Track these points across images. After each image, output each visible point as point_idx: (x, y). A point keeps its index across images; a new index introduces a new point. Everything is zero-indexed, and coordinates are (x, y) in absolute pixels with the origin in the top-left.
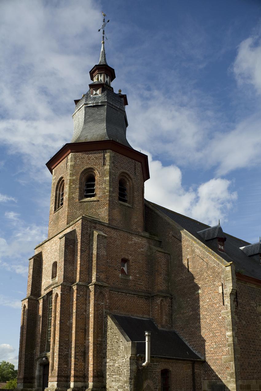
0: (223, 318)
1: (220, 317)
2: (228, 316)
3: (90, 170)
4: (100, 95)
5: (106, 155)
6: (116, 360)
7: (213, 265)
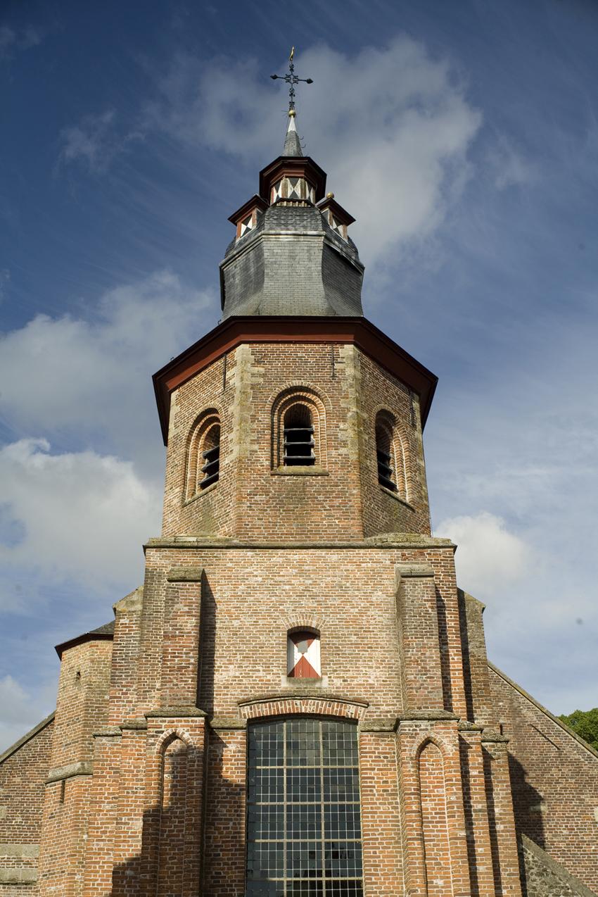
7: (577, 757)
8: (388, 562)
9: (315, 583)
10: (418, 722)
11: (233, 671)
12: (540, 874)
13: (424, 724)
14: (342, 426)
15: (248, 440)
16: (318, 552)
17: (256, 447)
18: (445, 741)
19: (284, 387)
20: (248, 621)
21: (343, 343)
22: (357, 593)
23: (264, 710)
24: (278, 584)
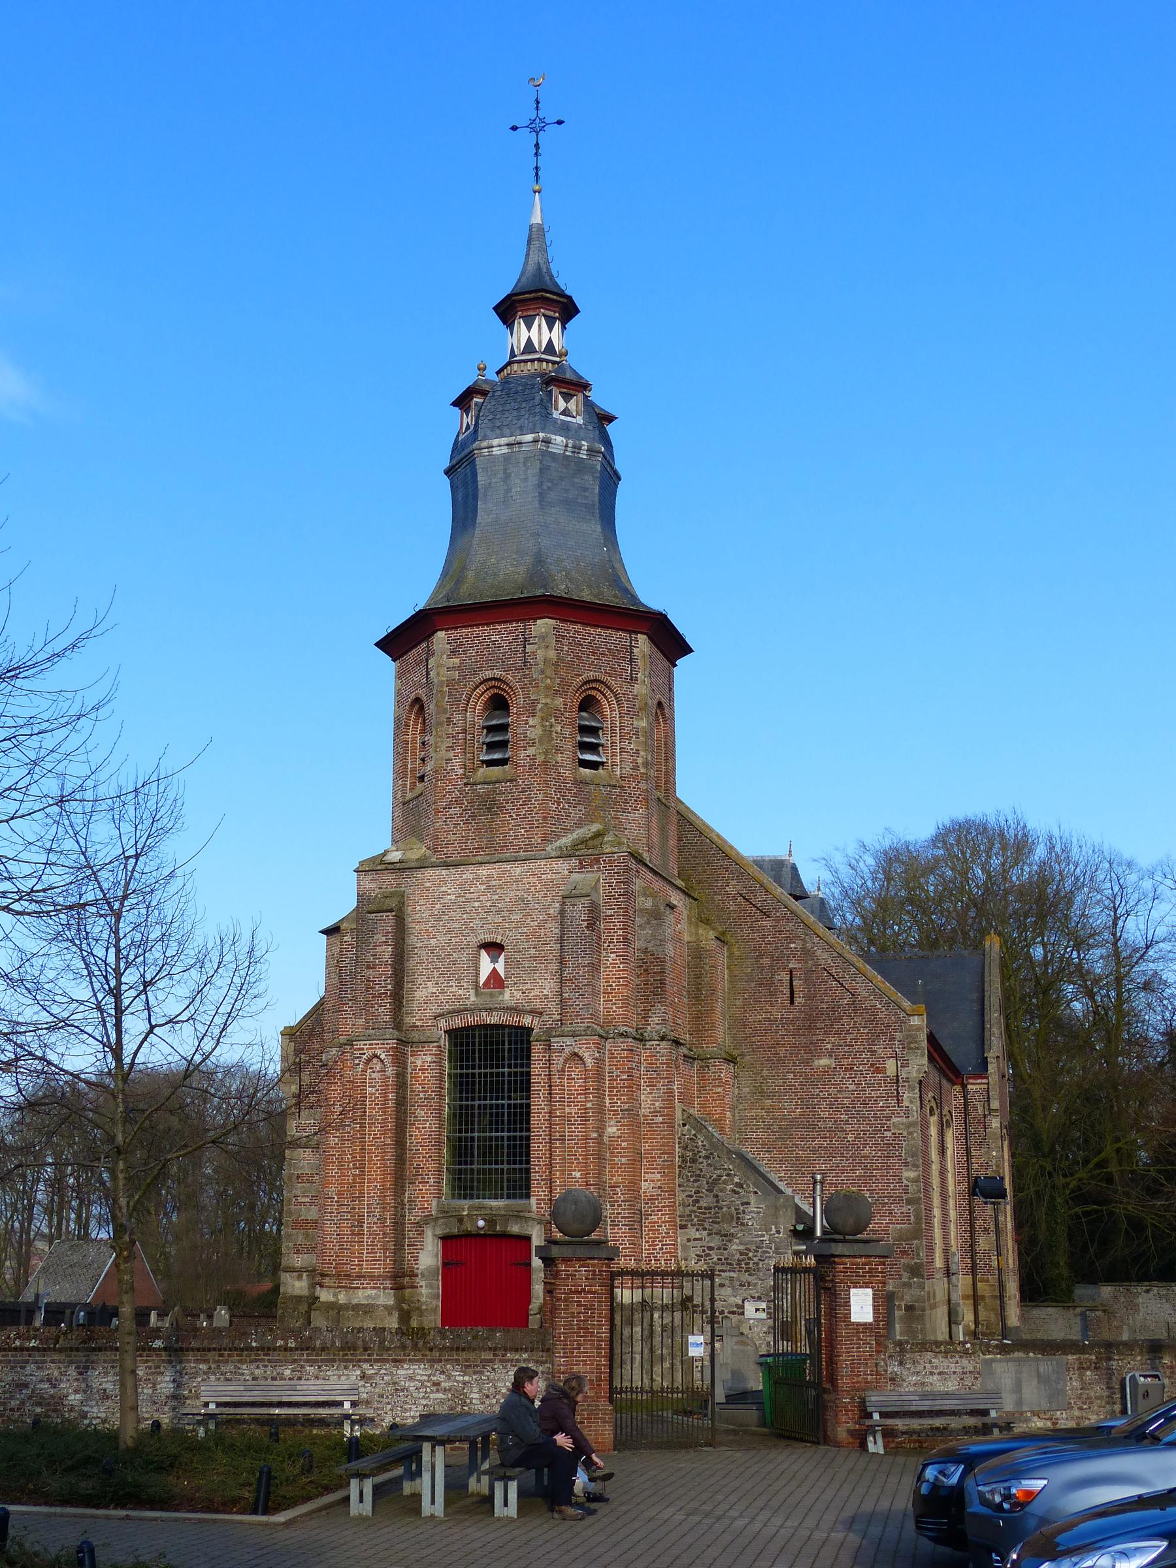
1: (888, 1134)
2: (910, 1133)
4: (579, 420)
5: (635, 650)
8: (566, 872)
9: (501, 899)
10: (565, 1039)
11: (431, 988)
12: (707, 1157)
13: (569, 1041)
14: (531, 723)
15: (444, 747)
16: (504, 865)
17: (451, 754)
18: (586, 1055)
19: (478, 679)
20: (443, 939)
21: (535, 619)
22: (537, 906)
23: (457, 1023)
24: (469, 901)
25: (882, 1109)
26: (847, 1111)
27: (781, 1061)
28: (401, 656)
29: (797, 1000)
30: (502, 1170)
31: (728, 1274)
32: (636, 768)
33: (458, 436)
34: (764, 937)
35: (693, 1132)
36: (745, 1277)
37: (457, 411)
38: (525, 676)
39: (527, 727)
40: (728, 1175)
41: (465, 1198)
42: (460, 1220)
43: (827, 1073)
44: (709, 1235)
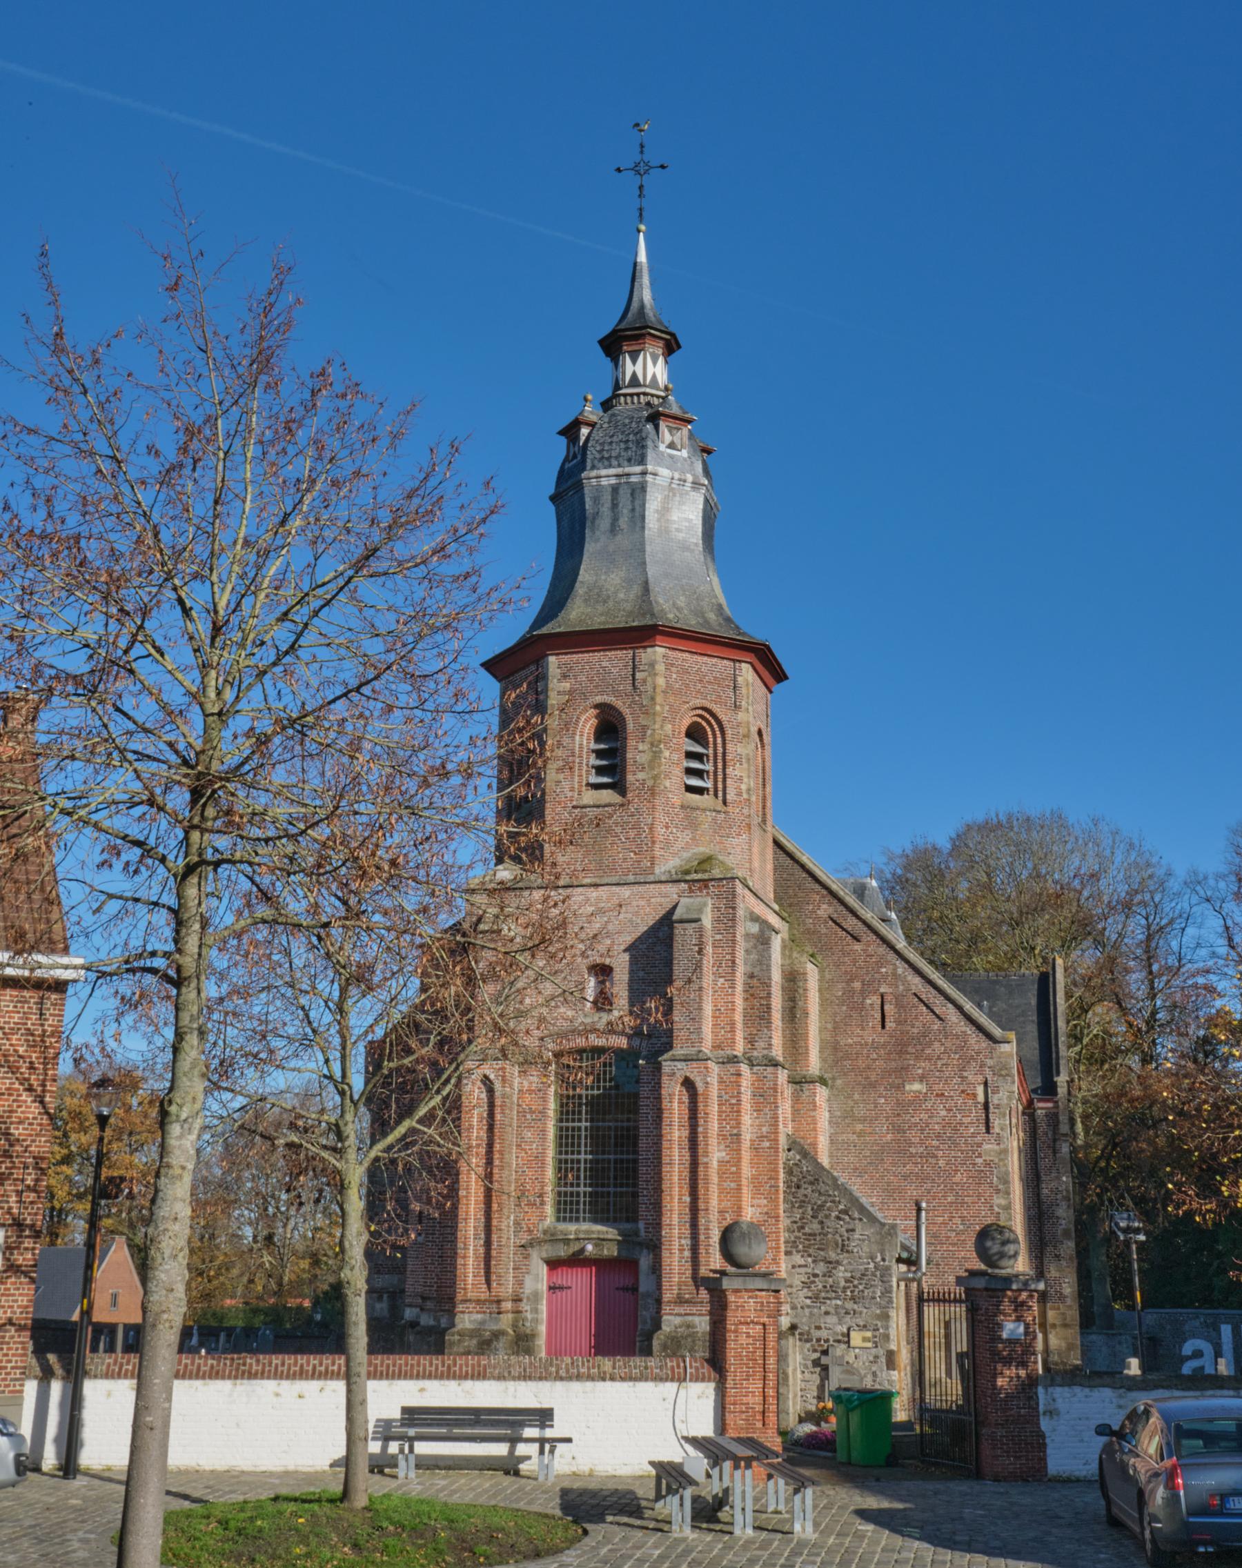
0: (987, 1164)
1: (979, 1161)
3: (700, 712)
5: (739, 679)
6: (838, 1263)
12: (811, 1183)
13: (679, 1065)
14: (641, 748)
17: (561, 776)
25: (973, 1135)
26: (938, 1136)
27: (873, 1085)
28: (508, 677)
29: (889, 1025)
30: (609, 1193)
31: (834, 1302)
32: (739, 794)
33: (563, 464)
34: (854, 961)
35: (798, 1157)
36: (850, 1305)
37: (563, 441)
38: (634, 702)
39: (637, 752)
40: (833, 1202)
41: (571, 1220)
42: (567, 1241)
43: (919, 1099)
44: (814, 1261)
